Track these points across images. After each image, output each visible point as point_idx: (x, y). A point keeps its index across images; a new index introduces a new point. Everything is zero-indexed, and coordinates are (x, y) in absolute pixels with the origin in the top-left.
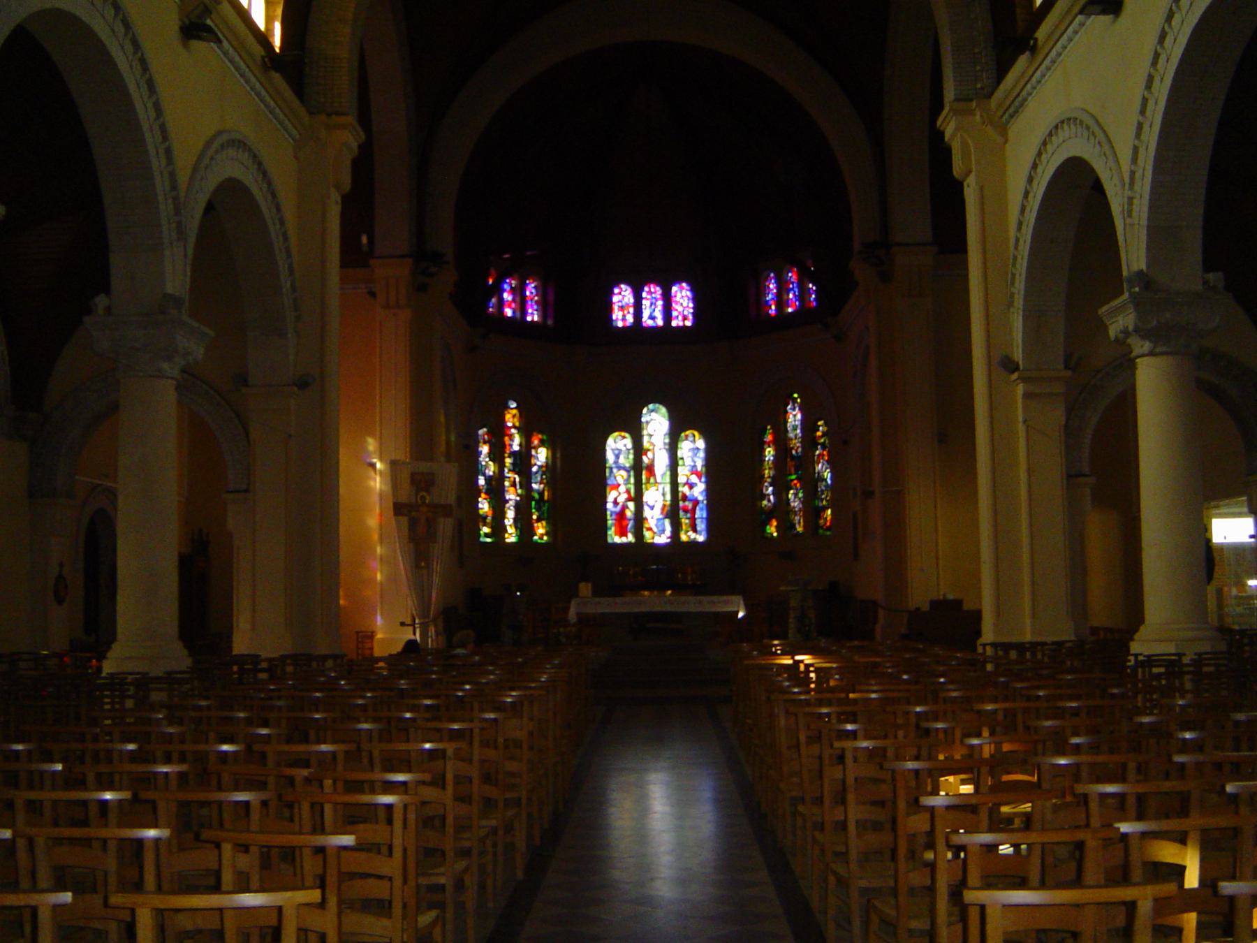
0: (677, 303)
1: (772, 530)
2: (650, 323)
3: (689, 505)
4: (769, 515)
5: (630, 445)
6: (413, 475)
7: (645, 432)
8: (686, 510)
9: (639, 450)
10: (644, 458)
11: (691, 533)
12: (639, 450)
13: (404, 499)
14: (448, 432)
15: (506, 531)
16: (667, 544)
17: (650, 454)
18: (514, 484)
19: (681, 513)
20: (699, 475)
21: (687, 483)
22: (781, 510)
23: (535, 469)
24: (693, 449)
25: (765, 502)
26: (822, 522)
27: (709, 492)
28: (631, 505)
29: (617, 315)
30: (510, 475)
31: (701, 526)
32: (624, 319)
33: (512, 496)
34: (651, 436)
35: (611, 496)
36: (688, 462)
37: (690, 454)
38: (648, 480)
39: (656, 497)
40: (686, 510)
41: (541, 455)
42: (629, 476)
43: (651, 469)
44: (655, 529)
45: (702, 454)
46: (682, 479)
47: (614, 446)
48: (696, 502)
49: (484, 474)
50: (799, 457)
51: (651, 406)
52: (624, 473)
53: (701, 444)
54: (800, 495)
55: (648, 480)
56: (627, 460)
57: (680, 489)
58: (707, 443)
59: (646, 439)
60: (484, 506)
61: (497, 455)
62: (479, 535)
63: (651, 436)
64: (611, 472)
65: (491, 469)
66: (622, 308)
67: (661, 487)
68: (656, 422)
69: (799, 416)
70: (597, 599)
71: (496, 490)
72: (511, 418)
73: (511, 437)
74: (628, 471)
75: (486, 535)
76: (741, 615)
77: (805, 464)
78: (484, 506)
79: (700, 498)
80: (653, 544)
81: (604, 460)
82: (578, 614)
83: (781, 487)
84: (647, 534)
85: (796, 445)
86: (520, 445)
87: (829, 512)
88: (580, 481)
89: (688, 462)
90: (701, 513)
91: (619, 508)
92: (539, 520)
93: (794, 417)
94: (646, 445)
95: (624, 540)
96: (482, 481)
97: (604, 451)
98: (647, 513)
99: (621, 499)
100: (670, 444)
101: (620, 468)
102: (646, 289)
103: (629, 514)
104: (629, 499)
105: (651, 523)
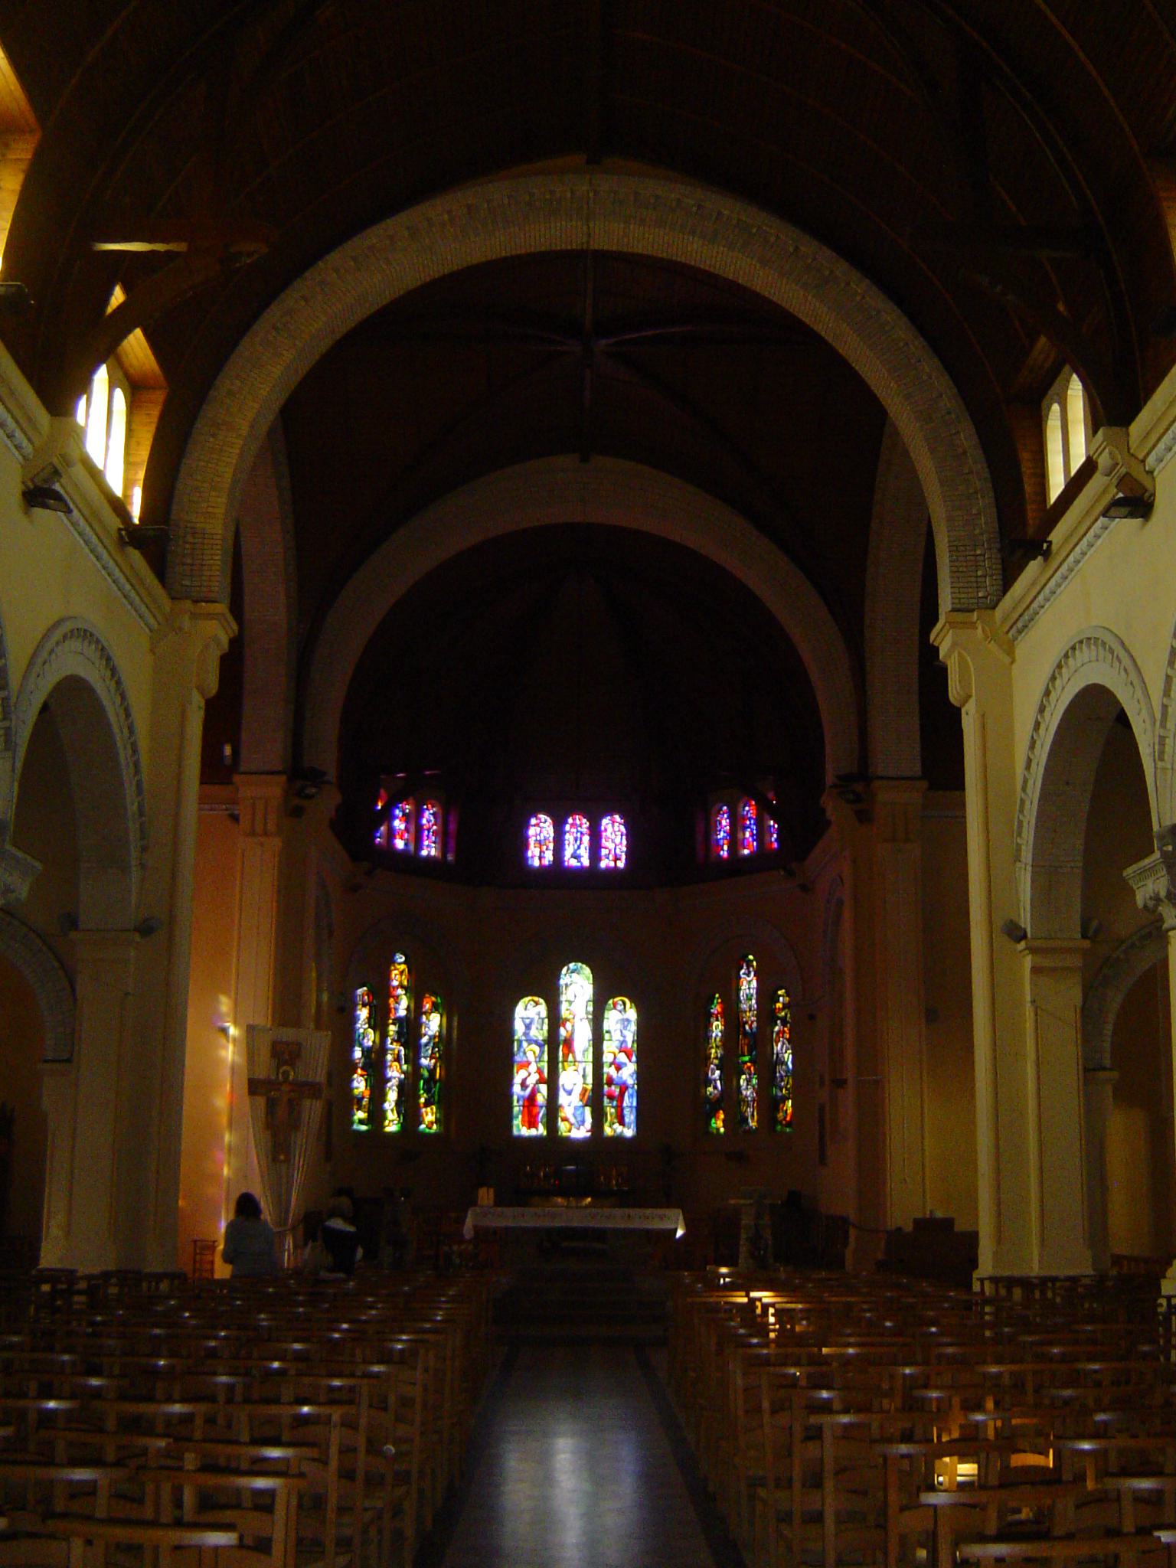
1: (718, 1124)
2: (574, 863)
3: (616, 1091)
4: (715, 1106)
5: (544, 1013)
6: (275, 1045)
7: (563, 998)
8: (611, 1097)
9: (555, 1020)
11: (616, 1126)
12: (555, 1020)
13: (261, 1073)
14: (319, 992)
17: (568, 1025)
18: (398, 1059)
19: (606, 1100)
22: (730, 1099)
23: (424, 1040)
24: (622, 1021)
25: (710, 1089)
26: (780, 1115)
27: (640, 1075)
28: (544, 1088)
29: (533, 851)
30: (395, 1046)
31: (630, 1117)
33: (395, 1073)
34: (570, 1002)
37: (619, 1026)
39: (574, 1079)
40: (611, 1097)
41: (433, 1024)
42: (542, 1052)
43: (569, 1043)
44: (572, 1120)
45: (633, 1027)
46: (607, 1058)
47: (525, 1014)
48: (624, 1088)
49: (361, 1045)
51: (572, 965)
52: (537, 1049)
53: (632, 1014)
54: (754, 1081)
55: (565, 1060)
56: (540, 1032)
57: (606, 1069)
58: (638, 1012)
59: (564, 1007)
60: (360, 1085)
61: (378, 1022)
63: (570, 1002)
64: (520, 1045)
65: (370, 1038)
66: (540, 843)
67: (581, 1067)
68: (577, 985)
69: (754, 984)
70: (499, 1209)
71: (375, 1066)
72: (398, 974)
73: (397, 998)
74: (541, 1046)
75: (361, 1122)
76: (680, 1233)
77: (760, 1042)
78: (360, 1085)
79: (630, 1081)
80: (568, 1138)
81: (510, 1032)
82: (475, 1227)
83: (730, 1069)
84: (563, 1127)
85: (750, 1019)
86: (408, 1009)
87: (790, 1103)
89: (617, 1036)
90: (630, 1101)
92: (427, 1104)
93: (749, 985)
94: (564, 1014)
95: (533, 1132)
96: (358, 1053)
98: (563, 1099)
99: (531, 1081)
101: (530, 1041)
102: (570, 820)
103: (541, 1099)
104: (541, 1081)
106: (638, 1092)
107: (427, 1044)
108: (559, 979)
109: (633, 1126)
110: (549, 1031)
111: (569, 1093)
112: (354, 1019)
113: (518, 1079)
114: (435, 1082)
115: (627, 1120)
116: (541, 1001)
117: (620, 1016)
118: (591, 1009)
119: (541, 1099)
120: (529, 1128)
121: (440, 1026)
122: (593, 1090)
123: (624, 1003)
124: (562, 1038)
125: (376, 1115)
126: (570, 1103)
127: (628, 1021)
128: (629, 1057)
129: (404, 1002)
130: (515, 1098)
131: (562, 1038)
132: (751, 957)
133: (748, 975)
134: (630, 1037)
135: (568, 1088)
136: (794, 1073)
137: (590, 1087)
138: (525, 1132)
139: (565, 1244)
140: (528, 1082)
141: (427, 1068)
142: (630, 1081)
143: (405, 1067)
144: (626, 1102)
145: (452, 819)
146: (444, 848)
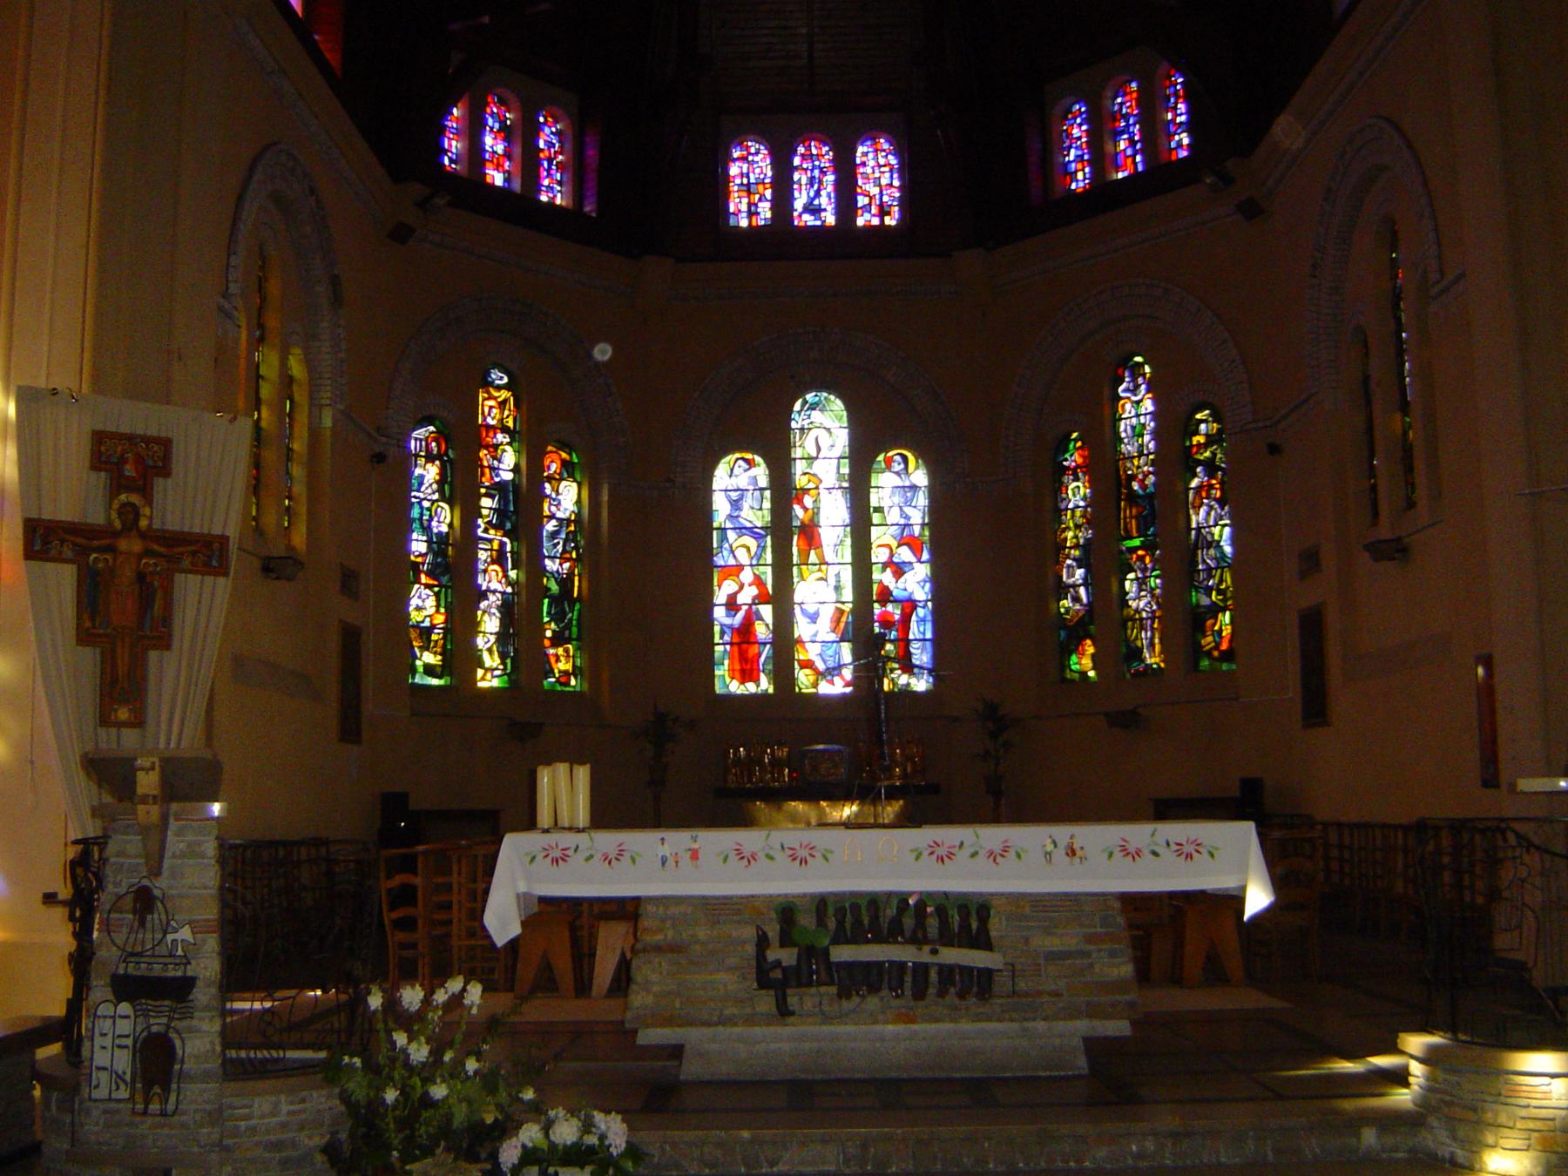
0: (866, 177)
1: (1083, 662)
2: (808, 219)
3: (895, 611)
4: (1076, 633)
5: (763, 481)
6: (99, 437)
7: (797, 453)
9: (783, 491)
12: (783, 491)
13: (63, 509)
14: (315, 406)
15: (481, 664)
16: (843, 697)
18: (499, 558)
20: (913, 544)
21: (885, 565)
23: (550, 526)
24: (904, 490)
25: (1066, 603)
26: (1208, 641)
27: (938, 581)
28: (766, 611)
29: (738, 203)
30: (492, 531)
31: (921, 655)
32: (752, 214)
33: (493, 581)
37: (897, 499)
38: (805, 555)
39: (821, 595)
41: (567, 498)
43: (810, 533)
45: (922, 500)
46: (879, 555)
48: (910, 605)
49: (427, 529)
50: (1150, 497)
51: (810, 397)
53: (920, 477)
54: (1153, 582)
55: (805, 555)
56: (757, 514)
57: (876, 576)
59: (800, 467)
60: (424, 605)
61: (460, 486)
62: (414, 671)
64: (724, 538)
65: (445, 519)
66: (748, 189)
67: (832, 570)
68: (823, 430)
69: (1148, 406)
70: (608, 840)
71: (453, 568)
72: (494, 407)
74: (757, 537)
75: (429, 670)
76: (1258, 899)
77: (1161, 511)
78: (424, 605)
81: (708, 512)
82: (523, 899)
83: (1105, 563)
84: (804, 679)
85: (1143, 474)
86: (516, 469)
87: (1227, 617)
89: (894, 516)
90: (921, 629)
92: (558, 640)
93: (1137, 410)
94: (801, 481)
95: (751, 688)
96: (419, 545)
97: (708, 492)
98: (802, 628)
99: (745, 598)
101: (741, 530)
102: (801, 150)
103: (762, 631)
104: (762, 598)
105: (812, 652)
106: (934, 612)
107: (554, 535)
108: (790, 419)
110: (773, 511)
111: (813, 618)
112: (404, 481)
113: (721, 597)
114: (572, 602)
116: (758, 459)
117: (897, 481)
118: (845, 470)
120: (743, 682)
121: (578, 502)
122: (853, 611)
123: (905, 459)
124: (796, 523)
125: (460, 657)
127: (914, 488)
128: (917, 552)
129: (509, 458)
130: (717, 629)
131: (796, 523)
132: (1139, 359)
133: (1134, 391)
134: (917, 517)
135: (811, 609)
136: (1237, 565)
137: (848, 607)
138: (735, 687)
139: (843, 954)
140: (740, 599)
141: (556, 576)
142: (921, 594)
143: (513, 574)
146: (578, 195)
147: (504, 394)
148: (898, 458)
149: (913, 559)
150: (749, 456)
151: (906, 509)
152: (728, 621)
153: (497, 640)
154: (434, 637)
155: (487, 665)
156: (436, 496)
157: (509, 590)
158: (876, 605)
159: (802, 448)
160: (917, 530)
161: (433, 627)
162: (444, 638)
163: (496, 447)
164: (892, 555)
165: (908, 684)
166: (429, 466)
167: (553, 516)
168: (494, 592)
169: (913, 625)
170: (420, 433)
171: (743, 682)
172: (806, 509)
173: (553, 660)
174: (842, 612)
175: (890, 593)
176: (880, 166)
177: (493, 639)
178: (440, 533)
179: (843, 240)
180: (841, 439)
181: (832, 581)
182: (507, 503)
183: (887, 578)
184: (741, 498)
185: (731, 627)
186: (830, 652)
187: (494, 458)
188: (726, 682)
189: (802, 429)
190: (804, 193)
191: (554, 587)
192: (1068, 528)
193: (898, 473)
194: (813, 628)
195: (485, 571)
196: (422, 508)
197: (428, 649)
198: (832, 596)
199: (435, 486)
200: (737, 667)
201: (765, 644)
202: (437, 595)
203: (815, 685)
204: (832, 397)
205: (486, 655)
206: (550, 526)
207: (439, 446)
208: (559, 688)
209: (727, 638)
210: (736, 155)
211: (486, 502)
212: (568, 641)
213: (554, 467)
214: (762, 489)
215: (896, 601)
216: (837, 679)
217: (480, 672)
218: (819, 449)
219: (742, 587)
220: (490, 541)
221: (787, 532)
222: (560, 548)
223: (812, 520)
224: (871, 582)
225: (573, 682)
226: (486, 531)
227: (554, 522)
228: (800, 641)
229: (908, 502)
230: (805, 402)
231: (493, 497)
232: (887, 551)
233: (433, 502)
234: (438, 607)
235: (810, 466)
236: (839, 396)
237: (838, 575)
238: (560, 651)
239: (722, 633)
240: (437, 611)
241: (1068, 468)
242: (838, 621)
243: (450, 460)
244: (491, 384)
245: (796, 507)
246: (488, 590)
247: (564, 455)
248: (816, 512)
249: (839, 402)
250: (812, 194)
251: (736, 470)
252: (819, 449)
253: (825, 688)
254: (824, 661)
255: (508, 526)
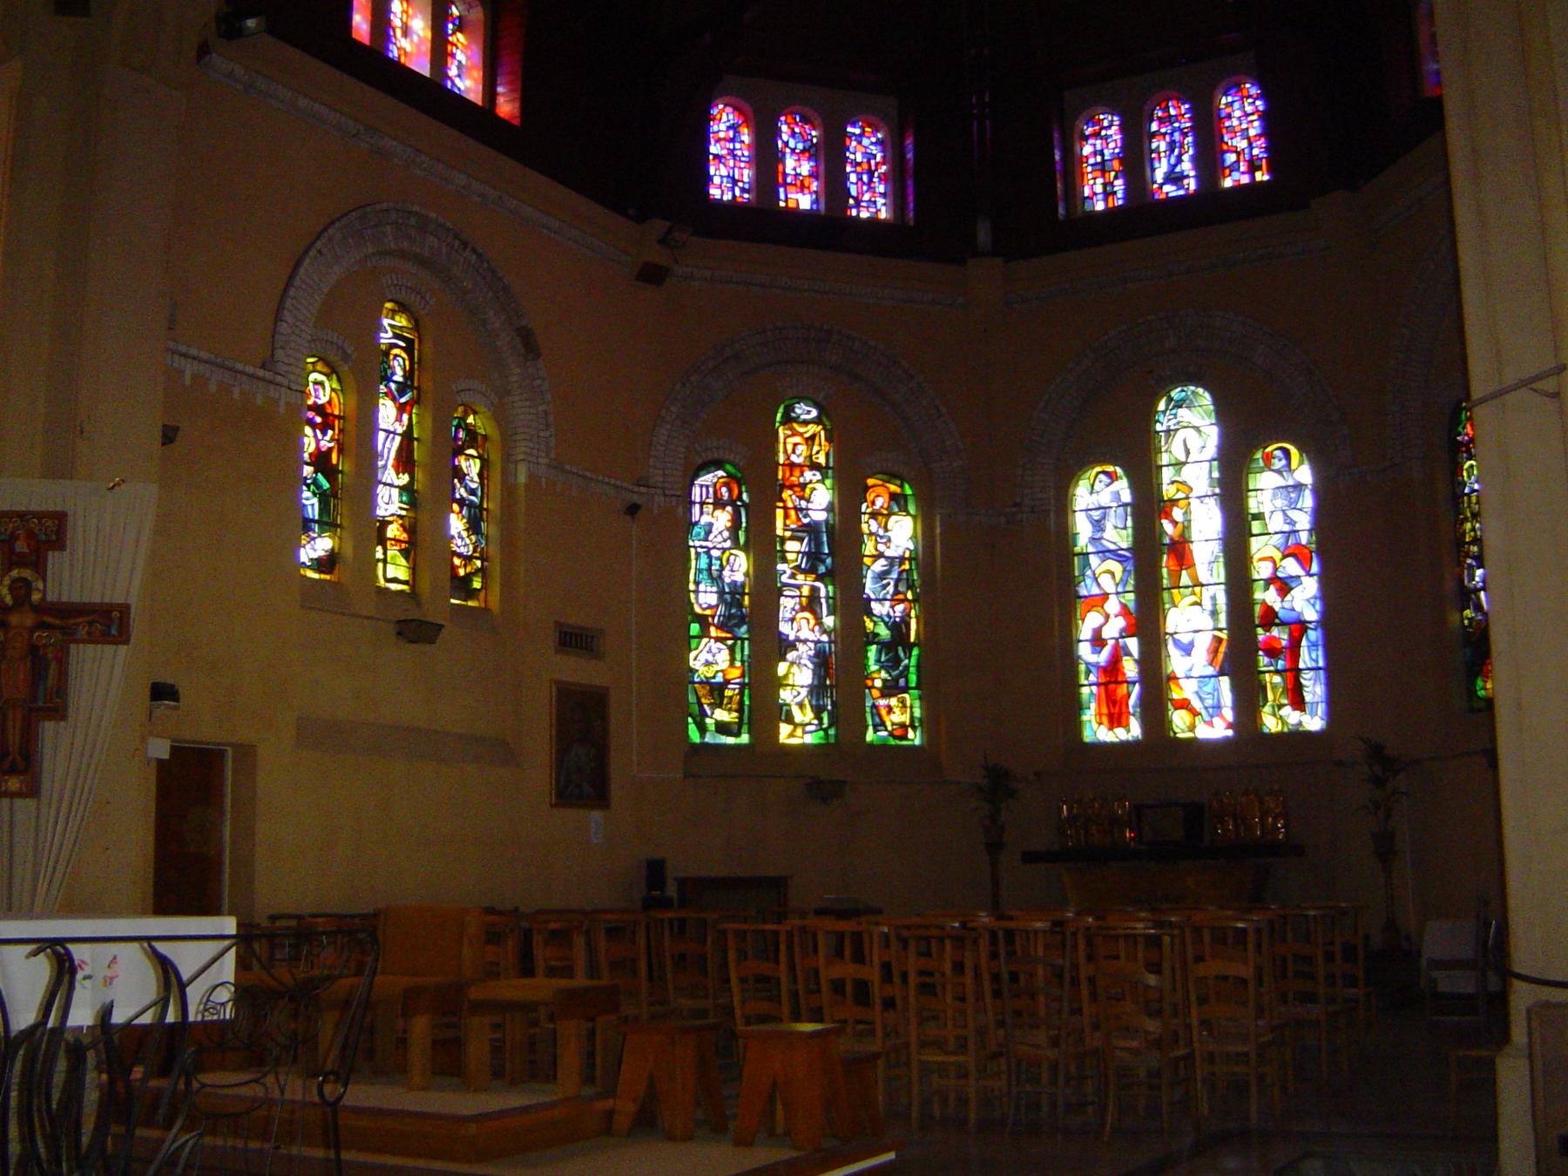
0: (1231, 130)
3: (1281, 635)
5: (1126, 497)
7: (1165, 459)
9: (1149, 507)
10: (1167, 526)
11: (1287, 711)
12: (1149, 507)
16: (1226, 741)
17: (1177, 514)
19: (1263, 660)
21: (1268, 582)
24: (1284, 492)
28: (1133, 644)
30: (801, 577)
31: (1314, 690)
32: (1108, 193)
33: (803, 629)
34: (1178, 465)
35: (1088, 625)
36: (1276, 523)
37: (1279, 503)
39: (1194, 621)
40: (1273, 653)
43: (1180, 551)
45: (1308, 501)
46: (1261, 571)
47: (1092, 501)
48: (1299, 628)
49: (717, 579)
52: (1117, 568)
53: (1304, 473)
56: (1119, 536)
57: (1259, 595)
59: (1167, 474)
60: (711, 658)
63: (1178, 465)
64: (1087, 565)
66: (1102, 168)
67: (1207, 593)
68: (1190, 431)
71: (751, 617)
74: (1122, 560)
75: (722, 728)
79: (1311, 615)
80: (1193, 743)
81: (1065, 536)
84: (1179, 721)
86: (829, 509)
88: (1000, 588)
89: (1276, 523)
90: (1310, 656)
91: (1103, 657)
92: (890, 689)
94: (1169, 491)
95: (1120, 735)
98: (1176, 662)
100: (1222, 482)
101: (1105, 553)
103: (1130, 668)
104: (1127, 632)
105: (1185, 690)
107: (882, 576)
109: (1321, 709)
111: (1187, 649)
113: (1085, 632)
114: (909, 648)
115: (1308, 697)
117: (1278, 481)
118: (1216, 474)
119: (1130, 668)
120: (1111, 728)
124: (1167, 541)
126: (1193, 669)
127: (1299, 487)
128: (1305, 563)
130: (1082, 667)
134: (1303, 521)
135: (1185, 639)
140: (1105, 634)
142: (1311, 615)
143: (829, 621)
144: (1305, 660)
145: (909, 142)
146: (898, 205)
147: (812, 429)
148: (1278, 453)
149: (1301, 573)
150: (1110, 469)
151: (1291, 514)
152: (1093, 658)
153: (810, 693)
154: (728, 693)
155: (797, 720)
156: (728, 544)
157: (825, 638)
158: (1260, 630)
159: (1171, 451)
160: (1304, 538)
161: (727, 682)
162: (741, 694)
163: (803, 486)
164: (1276, 569)
165: (1300, 724)
166: (718, 513)
167: (881, 555)
168: (805, 642)
169: (1304, 651)
170: (707, 479)
171: (1111, 728)
172: (1175, 523)
173: (884, 712)
174: (1219, 640)
175: (1275, 614)
176: (1247, 115)
177: (804, 692)
178: (734, 582)
179: (1211, 205)
180: (1212, 435)
181: (1207, 604)
182: (819, 544)
183: (1271, 597)
184: (1104, 517)
185: (1097, 665)
186: (1208, 689)
187: (801, 498)
188: (1096, 730)
189: (1168, 431)
190: (1164, 161)
191: (884, 632)
192: (1466, 519)
193: (1278, 472)
194: (1187, 661)
195: (792, 620)
196: (710, 557)
197: (720, 706)
198: (1210, 624)
199: (726, 534)
200: (1105, 711)
201: (1134, 683)
202: (732, 649)
203: (1192, 728)
204: (1200, 390)
205: (795, 711)
206: (879, 566)
207: (730, 491)
208: (892, 742)
209: (1092, 678)
210: (1089, 131)
211: (792, 546)
212: (906, 689)
213: (879, 502)
214: (1125, 505)
215: (1283, 623)
216: (1216, 720)
217: (785, 729)
218: (1188, 452)
219: (1107, 617)
220: (799, 587)
221: (1153, 556)
222: (891, 589)
223: (1182, 535)
224: (1252, 603)
225: (911, 734)
226: (793, 576)
227: (882, 561)
228: (1173, 678)
229: (1293, 505)
230: (1170, 399)
231: (801, 540)
232: (1269, 565)
233: (724, 550)
234: (733, 660)
235: (1178, 472)
236: (1206, 388)
237: (1214, 598)
238: (893, 701)
239: (1088, 672)
240: (732, 665)
241: (1461, 443)
242: (1215, 652)
243: (745, 505)
244: (796, 420)
245: (1164, 522)
246: (798, 640)
247: (893, 488)
248: (1187, 527)
249: (1207, 395)
250: (1173, 161)
251: (1097, 486)
252: (1188, 452)
253: (1204, 732)
254: (1201, 699)
255: (822, 569)
